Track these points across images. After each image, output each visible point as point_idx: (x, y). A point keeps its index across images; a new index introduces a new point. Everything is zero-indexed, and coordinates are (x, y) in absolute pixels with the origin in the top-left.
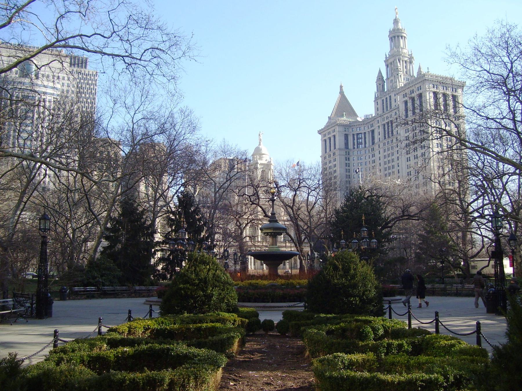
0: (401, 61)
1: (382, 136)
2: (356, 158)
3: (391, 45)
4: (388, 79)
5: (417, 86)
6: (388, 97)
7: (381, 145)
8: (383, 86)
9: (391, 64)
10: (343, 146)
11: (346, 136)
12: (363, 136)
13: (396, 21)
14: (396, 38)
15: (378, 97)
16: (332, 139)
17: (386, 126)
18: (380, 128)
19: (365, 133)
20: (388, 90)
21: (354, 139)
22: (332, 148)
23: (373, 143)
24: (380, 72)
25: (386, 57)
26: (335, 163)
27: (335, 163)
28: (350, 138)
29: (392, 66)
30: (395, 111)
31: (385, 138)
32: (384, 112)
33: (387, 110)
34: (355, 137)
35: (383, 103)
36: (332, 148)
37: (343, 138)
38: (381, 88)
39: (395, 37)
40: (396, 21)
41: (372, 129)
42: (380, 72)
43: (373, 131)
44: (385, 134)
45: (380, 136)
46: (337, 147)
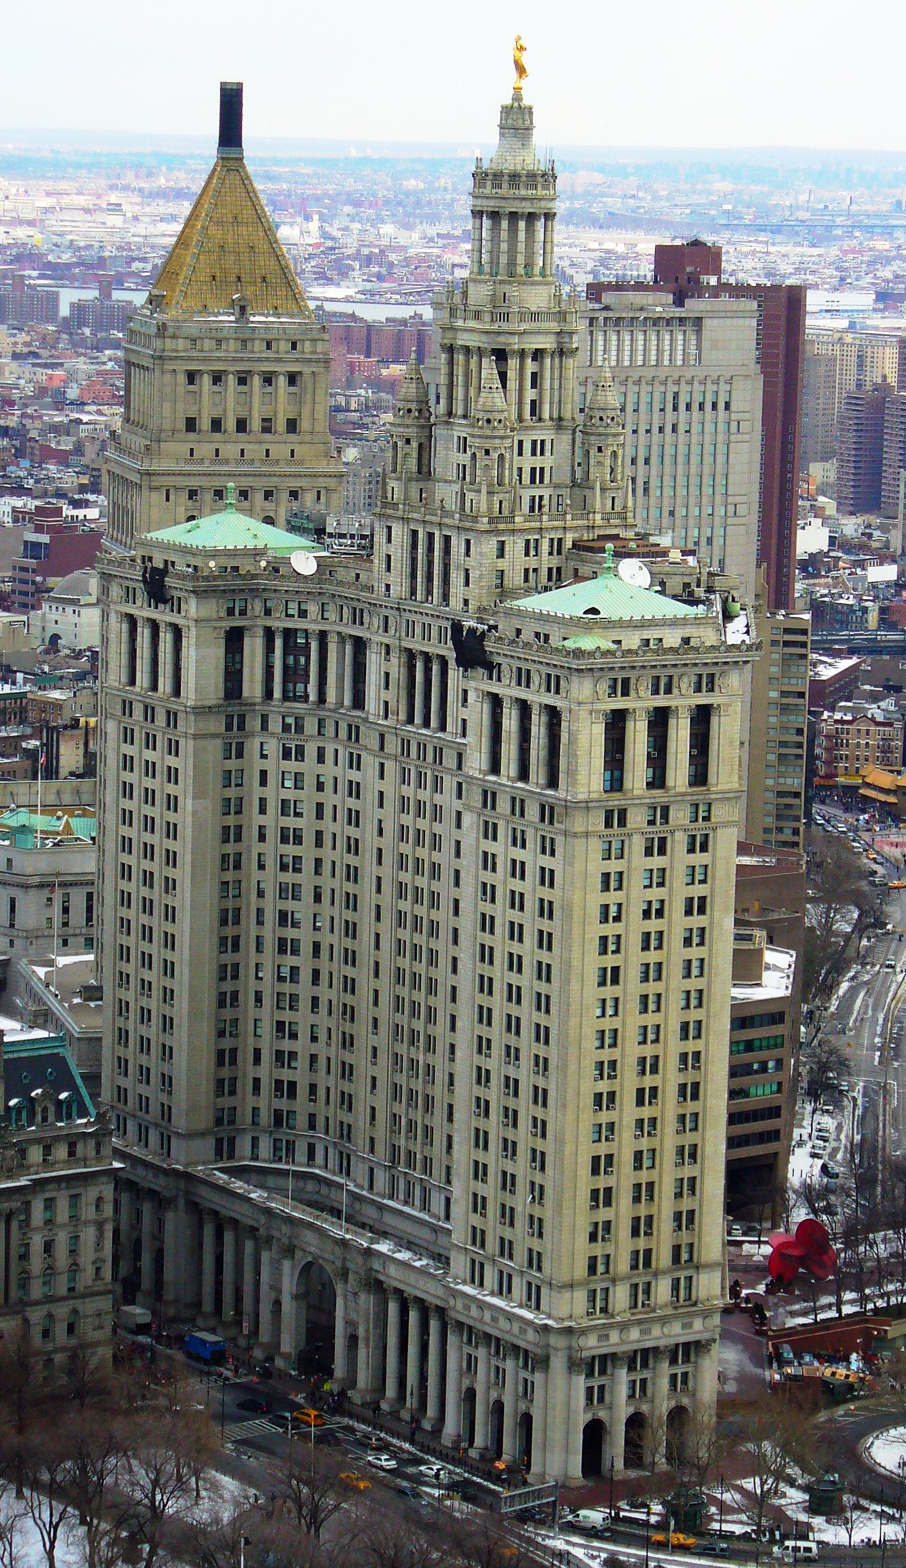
0: (513, 363)
1: (395, 696)
2: (273, 748)
10: (214, 689)
11: (234, 639)
12: (314, 646)
13: (516, 120)
18: (394, 660)
19: (323, 636)
21: (269, 649)
28: (253, 646)
32: (413, 592)
34: (279, 643)
35: (414, 546)
37: (218, 652)
40: (516, 120)
45: (390, 696)
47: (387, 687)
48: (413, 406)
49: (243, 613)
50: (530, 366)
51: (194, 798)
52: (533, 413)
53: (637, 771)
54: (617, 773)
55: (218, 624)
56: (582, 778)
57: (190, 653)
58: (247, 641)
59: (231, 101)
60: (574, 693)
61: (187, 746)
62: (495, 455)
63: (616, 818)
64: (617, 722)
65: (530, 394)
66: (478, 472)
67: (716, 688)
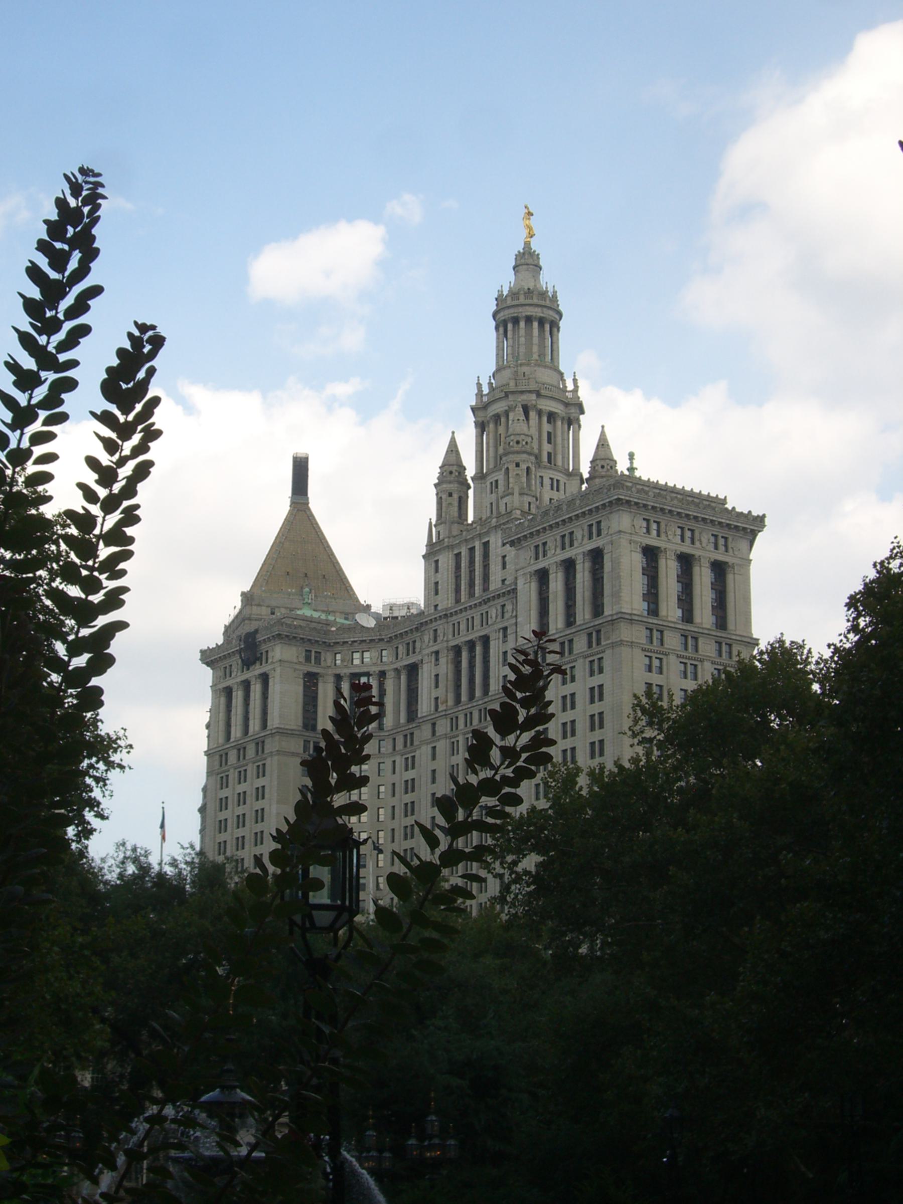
0: (533, 415)
1: (445, 691)
3: (500, 349)
4: (480, 477)
5: (585, 522)
6: (477, 545)
7: (443, 727)
8: (462, 502)
9: (497, 418)
11: (311, 681)
12: (374, 682)
13: (527, 261)
14: (522, 324)
15: (440, 541)
16: (256, 689)
17: (465, 655)
18: (443, 660)
19: (382, 674)
20: (478, 520)
22: (255, 725)
23: (412, 714)
24: (453, 449)
25: (480, 394)
26: (260, 783)
27: (260, 783)
29: (501, 429)
30: (501, 601)
31: (458, 700)
33: (471, 594)
35: (458, 567)
36: (255, 725)
37: (297, 689)
38: (455, 510)
39: (516, 321)
40: (527, 261)
41: (411, 660)
42: (453, 449)
43: (413, 670)
44: (458, 687)
46: (274, 721)
47: (437, 686)
48: (454, 468)
49: (318, 661)
50: (546, 428)
51: (278, 802)
52: (549, 461)
53: (671, 610)
54: (652, 606)
55: (298, 667)
56: (625, 595)
57: (275, 687)
58: (320, 685)
59: (301, 468)
60: (615, 527)
61: (272, 764)
62: (524, 466)
63: (656, 632)
64: (651, 554)
65: (547, 448)
66: (511, 480)
67: (730, 550)
